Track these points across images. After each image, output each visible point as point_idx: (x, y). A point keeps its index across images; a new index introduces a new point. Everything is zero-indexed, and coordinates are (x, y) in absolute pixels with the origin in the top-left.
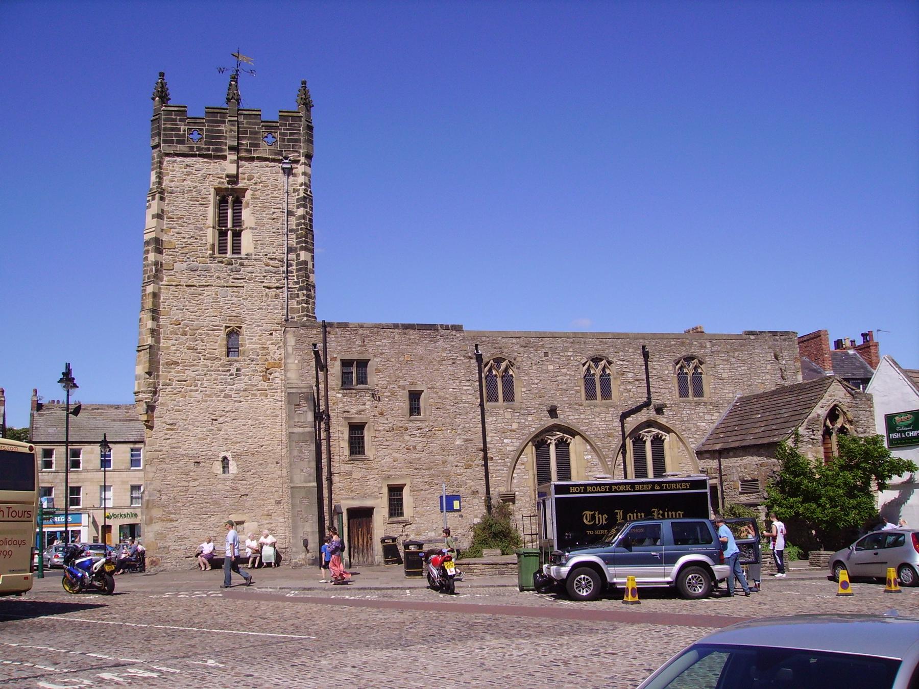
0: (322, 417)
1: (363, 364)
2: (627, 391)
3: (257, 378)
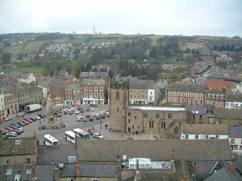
0: (125, 118)
1: (130, 113)
2: (161, 117)
3: (120, 113)
